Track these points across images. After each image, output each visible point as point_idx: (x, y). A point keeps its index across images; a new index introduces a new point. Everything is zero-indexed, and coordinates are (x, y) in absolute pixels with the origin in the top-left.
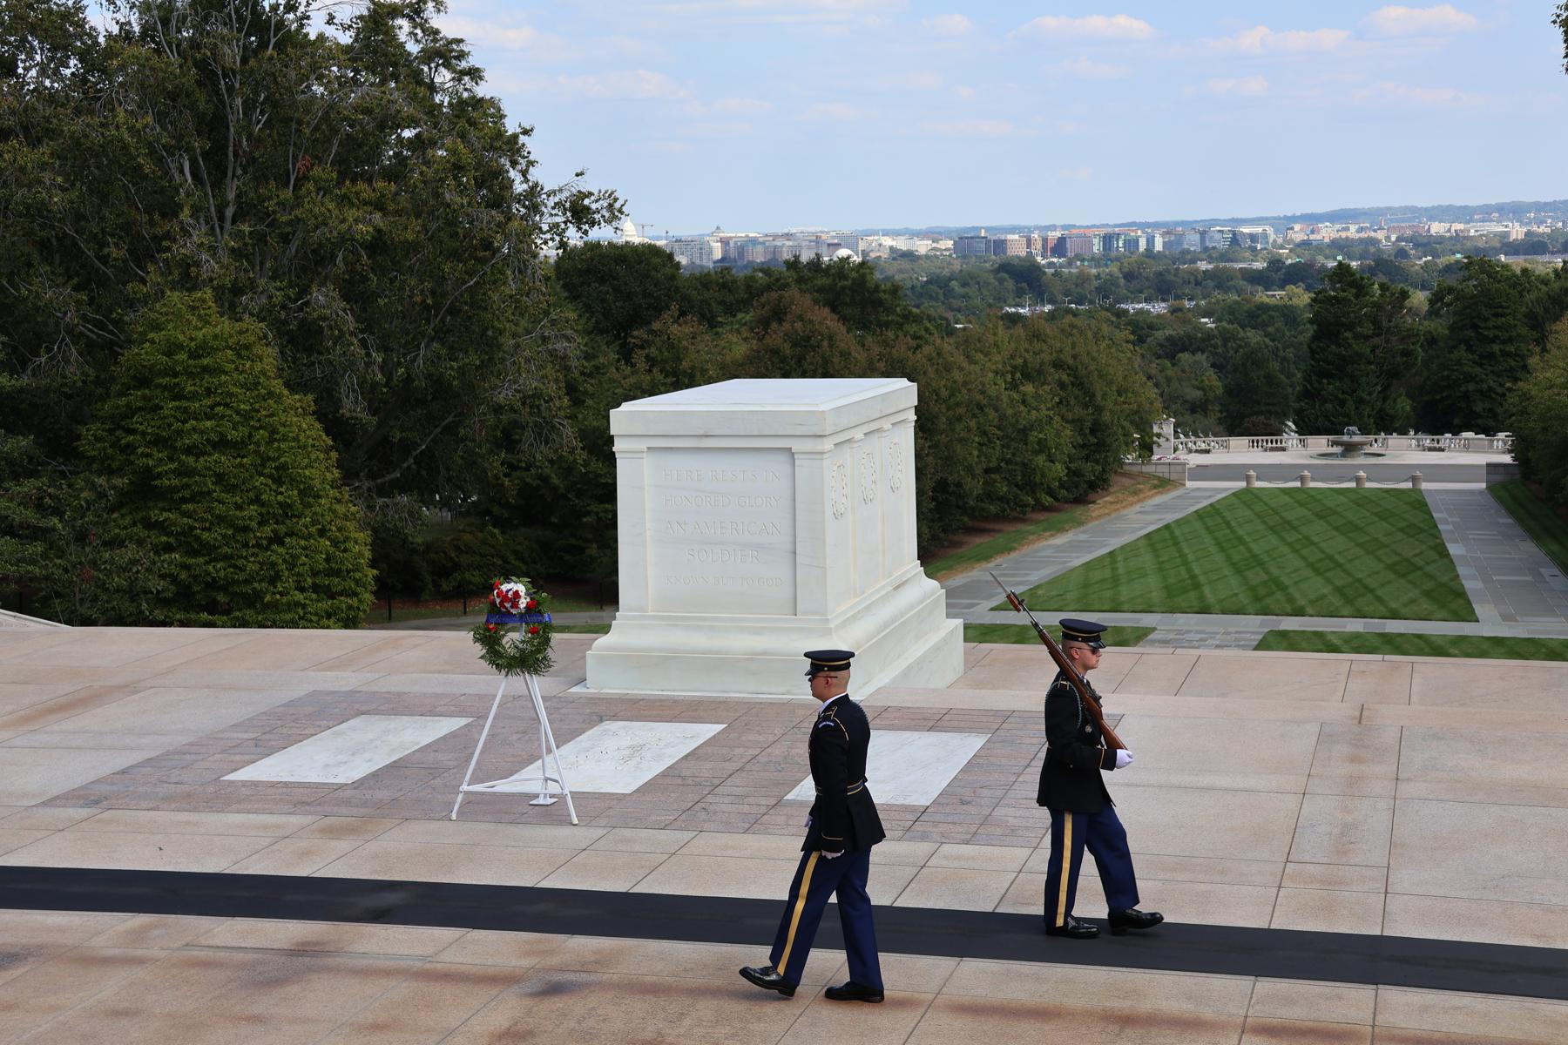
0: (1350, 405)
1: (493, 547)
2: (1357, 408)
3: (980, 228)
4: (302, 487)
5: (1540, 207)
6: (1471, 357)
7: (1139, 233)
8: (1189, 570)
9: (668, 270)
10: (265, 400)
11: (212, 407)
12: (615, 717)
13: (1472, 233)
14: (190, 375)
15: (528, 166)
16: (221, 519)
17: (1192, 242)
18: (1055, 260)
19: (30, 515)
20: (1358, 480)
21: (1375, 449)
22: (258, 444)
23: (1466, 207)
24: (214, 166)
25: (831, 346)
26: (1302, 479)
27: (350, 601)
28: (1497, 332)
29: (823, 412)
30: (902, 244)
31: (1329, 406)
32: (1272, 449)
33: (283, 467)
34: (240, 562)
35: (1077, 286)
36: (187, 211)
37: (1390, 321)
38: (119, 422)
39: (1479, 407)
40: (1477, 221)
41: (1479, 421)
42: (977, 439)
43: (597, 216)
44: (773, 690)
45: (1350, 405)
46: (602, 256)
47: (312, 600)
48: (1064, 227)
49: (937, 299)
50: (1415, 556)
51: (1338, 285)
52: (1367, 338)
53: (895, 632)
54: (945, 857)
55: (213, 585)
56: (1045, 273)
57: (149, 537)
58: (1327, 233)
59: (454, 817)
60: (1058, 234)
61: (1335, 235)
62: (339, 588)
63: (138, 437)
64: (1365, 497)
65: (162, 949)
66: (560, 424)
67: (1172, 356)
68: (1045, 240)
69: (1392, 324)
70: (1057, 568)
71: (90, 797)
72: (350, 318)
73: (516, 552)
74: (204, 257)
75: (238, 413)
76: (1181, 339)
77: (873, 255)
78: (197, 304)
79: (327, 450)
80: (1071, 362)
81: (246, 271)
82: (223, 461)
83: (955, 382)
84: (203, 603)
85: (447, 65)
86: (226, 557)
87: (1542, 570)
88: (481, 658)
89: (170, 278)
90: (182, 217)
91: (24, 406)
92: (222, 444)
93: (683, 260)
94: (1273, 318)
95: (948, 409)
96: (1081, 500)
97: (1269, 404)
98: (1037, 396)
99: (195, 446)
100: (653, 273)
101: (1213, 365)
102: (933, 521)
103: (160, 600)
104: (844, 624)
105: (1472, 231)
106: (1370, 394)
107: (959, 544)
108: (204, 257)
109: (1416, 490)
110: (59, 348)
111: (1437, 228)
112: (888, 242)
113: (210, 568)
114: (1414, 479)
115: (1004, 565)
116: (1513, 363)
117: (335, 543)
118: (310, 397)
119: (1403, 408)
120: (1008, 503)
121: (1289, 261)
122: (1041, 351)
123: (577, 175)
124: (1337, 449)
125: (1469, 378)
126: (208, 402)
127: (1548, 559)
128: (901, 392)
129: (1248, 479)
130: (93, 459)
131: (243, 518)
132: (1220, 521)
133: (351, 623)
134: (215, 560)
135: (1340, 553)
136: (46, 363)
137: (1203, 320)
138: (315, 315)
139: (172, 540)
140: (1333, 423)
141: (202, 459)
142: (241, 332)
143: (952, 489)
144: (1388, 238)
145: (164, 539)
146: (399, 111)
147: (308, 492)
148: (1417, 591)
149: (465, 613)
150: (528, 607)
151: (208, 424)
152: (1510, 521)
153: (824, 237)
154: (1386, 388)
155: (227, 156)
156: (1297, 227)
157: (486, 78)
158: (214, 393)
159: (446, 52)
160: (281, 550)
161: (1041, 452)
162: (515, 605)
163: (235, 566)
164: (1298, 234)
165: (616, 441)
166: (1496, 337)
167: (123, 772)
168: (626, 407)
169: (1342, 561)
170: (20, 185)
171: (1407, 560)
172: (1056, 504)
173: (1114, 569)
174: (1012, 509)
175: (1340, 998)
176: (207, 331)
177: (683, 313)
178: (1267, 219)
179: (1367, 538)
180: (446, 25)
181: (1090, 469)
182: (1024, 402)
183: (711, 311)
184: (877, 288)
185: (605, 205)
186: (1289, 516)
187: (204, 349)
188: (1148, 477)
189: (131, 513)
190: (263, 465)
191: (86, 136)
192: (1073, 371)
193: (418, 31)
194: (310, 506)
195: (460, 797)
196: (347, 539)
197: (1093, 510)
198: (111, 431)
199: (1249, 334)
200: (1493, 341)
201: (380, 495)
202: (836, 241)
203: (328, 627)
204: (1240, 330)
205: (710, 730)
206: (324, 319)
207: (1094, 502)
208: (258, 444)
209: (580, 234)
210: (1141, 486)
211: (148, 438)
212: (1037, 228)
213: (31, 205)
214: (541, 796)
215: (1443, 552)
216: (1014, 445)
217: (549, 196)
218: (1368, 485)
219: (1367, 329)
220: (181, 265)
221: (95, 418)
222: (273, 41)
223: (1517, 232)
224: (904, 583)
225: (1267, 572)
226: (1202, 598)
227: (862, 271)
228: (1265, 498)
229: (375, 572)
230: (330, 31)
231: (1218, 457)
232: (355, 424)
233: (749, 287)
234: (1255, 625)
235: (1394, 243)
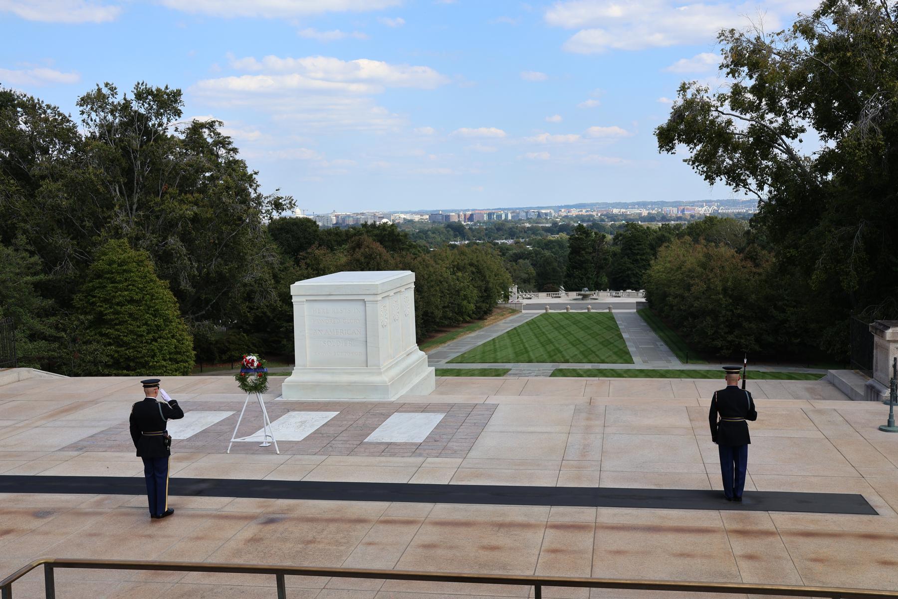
0: (585, 280)
2: (587, 281)
3: (439, 211)
4: (165, 318)
5: (653, 203)
6: (629, 261)
7: (502, 212)
8: (524, 346)
10: (149, 283)
11: (127, 286)
12: (294, 410)
13: (628, 213)
14: (119, 273)
15: (256, 187)
16: (132, 332)
17: (522, 215)
18: (469, 223)
19: (53, 332)
20: (588, 309)
21: (595, 297)
22: (146, 301)
23: (626, 203)
24: (129, 189)
25: (380, 258)
26: (567, 309)
27: (185, 365)
28: (638, 251)
29: (377, 284)
30: (408, 217)
31: (576, 280)
32: (555, 297)
33: (157, 310)
34: (139, 349)
35: (478, 233)
36: (117, 207)
37: (599, 247)
38: (90, 293)
39: (633, 280)
40: (630, 208)
41: (633, 286)
42: (439, 295)
43: (285, 207)
44: (358, 397)
45: (585, 280)
46: (287, 223)
47: (169, 364)
48: (473, 210)
49: (423, 239)
50: (611, 338)
51: (579, 233)
52: (590, 253)
53: (409, 372)
54: (429, 463)
55: (128, 359)
56: (465, 228)
57: (102, 339)
58: (574, 212)
59: (228, 452)
60: (470, 213)
61: (577, 213)
62: (180, 359)
63: (97, 299)
64: (591, 316)
65: (109, 509)
67: (516, 261)
68: (465, 215)
69: (600, 248)
71: (77, 447)
72: (184, 249)
74: (124, 225)
75: (138, 288)
76: (519, 254)
77: (397, 221)
79: (175, 303)
80: (476, 263)
81: (141, 230)
82: (132, 308)
83: (430, 272)
85: (224, 147)
86: (133, 347)
87: (657, 343)
88: (239, 387)
89: (110, 234)
90: (115, 209)
91: (50, 287)
92: (131, 301)
93: (320, 224)
94: (554, 245)
95: (428, 283)
96: (481, 318)
97: (553, 280)
98: (463, 277)
100: (308, 229)
101: (532, 264)
102: (422, 327)
103: (107, 366)
104: (387, 370)
105: (628, 212)
106: (592, 275)
107: (433, 337)
108: (124, 225)
109: (610, 313)
110: (65, 263)
111: (615, 211)
112: (403, 216)
114: (609, 308)
115: (451, 345)
116: (645, 263)
117: (178, 341)
118: (168, 281)
119: (604, 281)
120: (452, 320)
121: (560, 223)
122: (464, 259)
123: (277, 190)
124: (580, 297)
125: (629, 269)
126: (126, 284)
127: (659, 338)
128: (409, 276)
129: (546, 309)
130: (79, 308)
131: (140, 331)
132: (536, 326)
133: (185, 373)
134: (128, 349)
135: (582, 338)
136: (60, 269)
137: (528, 247)
138: (170, 248)
139: (111, 341)
140: (578, 287)
141: (123, 308)
142: (139, 256)
143: (430, 315)
144: (597, 215)
145: (108, 340)
146: (204, 166)
147: (167, 321)
148: (611, 352)
149: (232, 368)
151: (126, 293)
152: (645, 324)
153: (377, 214)
154: (598, 273)
155: (134, 184)
156: (563, 210)
157: (240, 152)
158: (128, 280)
159: (223, 142)
160: (156, 344)
161: (465, 299)
163: (137, 351)
164: (563, 213)
166: (638, 253)
167: (92, 436)
168: (297, 283)
169: (583, 341)
170: (49, 197)
171: (607, 340)
172: (471, 320)
173: (495, 346)
174: (454, 322)
175: (583, 512)
176: (125, 255)
177: (320, 245)
178: (551, 207)
179: (592, 332)
180: (223, 131)
181: (484, 306)
182: (458, 279)
183: (332, 245)
184: (398, 235)
185: (288, 202)
186: (562, 323)
187: (124, 262)
188: (507, 309)
189: (94, 330)
190: (149, 310)
191: (76, 178)
192: (477, 267)
193: (212, 134)
194: (168, 326)
195: (231, 444)
196: (183, 339)
197: (486, 322)
198: (86, 297)
199: (545, 252)
200: (638, 254)
201: (197, 321)
202: (382, 216)
203: (176, 375)
204: (542, 251)
205: (333, 414)
206: (174, 249)
207: (486, 319)
208: (146, 301)
209: (278, 214)
210: (505, 313)
211: (101, 299)
212: (462, 210)
214: (264, 443)
215: (621, 337)
216: (454, 297)
217: (265, 199)
218: (592, 311)
219: (590, 250)
220: (115, 229)
221: (79, 291)
222: (153, 138)
223: (645, 213)
224: (411, 353)
225: (554, 346)
226: (529, 357)
227: (392, 228)
228: (553, 317)
229: (195, 352)
230: (176, 134)
231: (535, 301)
232: (186, 292)
233: (347, 234)
234: (550, 367)
235: (599, 217)
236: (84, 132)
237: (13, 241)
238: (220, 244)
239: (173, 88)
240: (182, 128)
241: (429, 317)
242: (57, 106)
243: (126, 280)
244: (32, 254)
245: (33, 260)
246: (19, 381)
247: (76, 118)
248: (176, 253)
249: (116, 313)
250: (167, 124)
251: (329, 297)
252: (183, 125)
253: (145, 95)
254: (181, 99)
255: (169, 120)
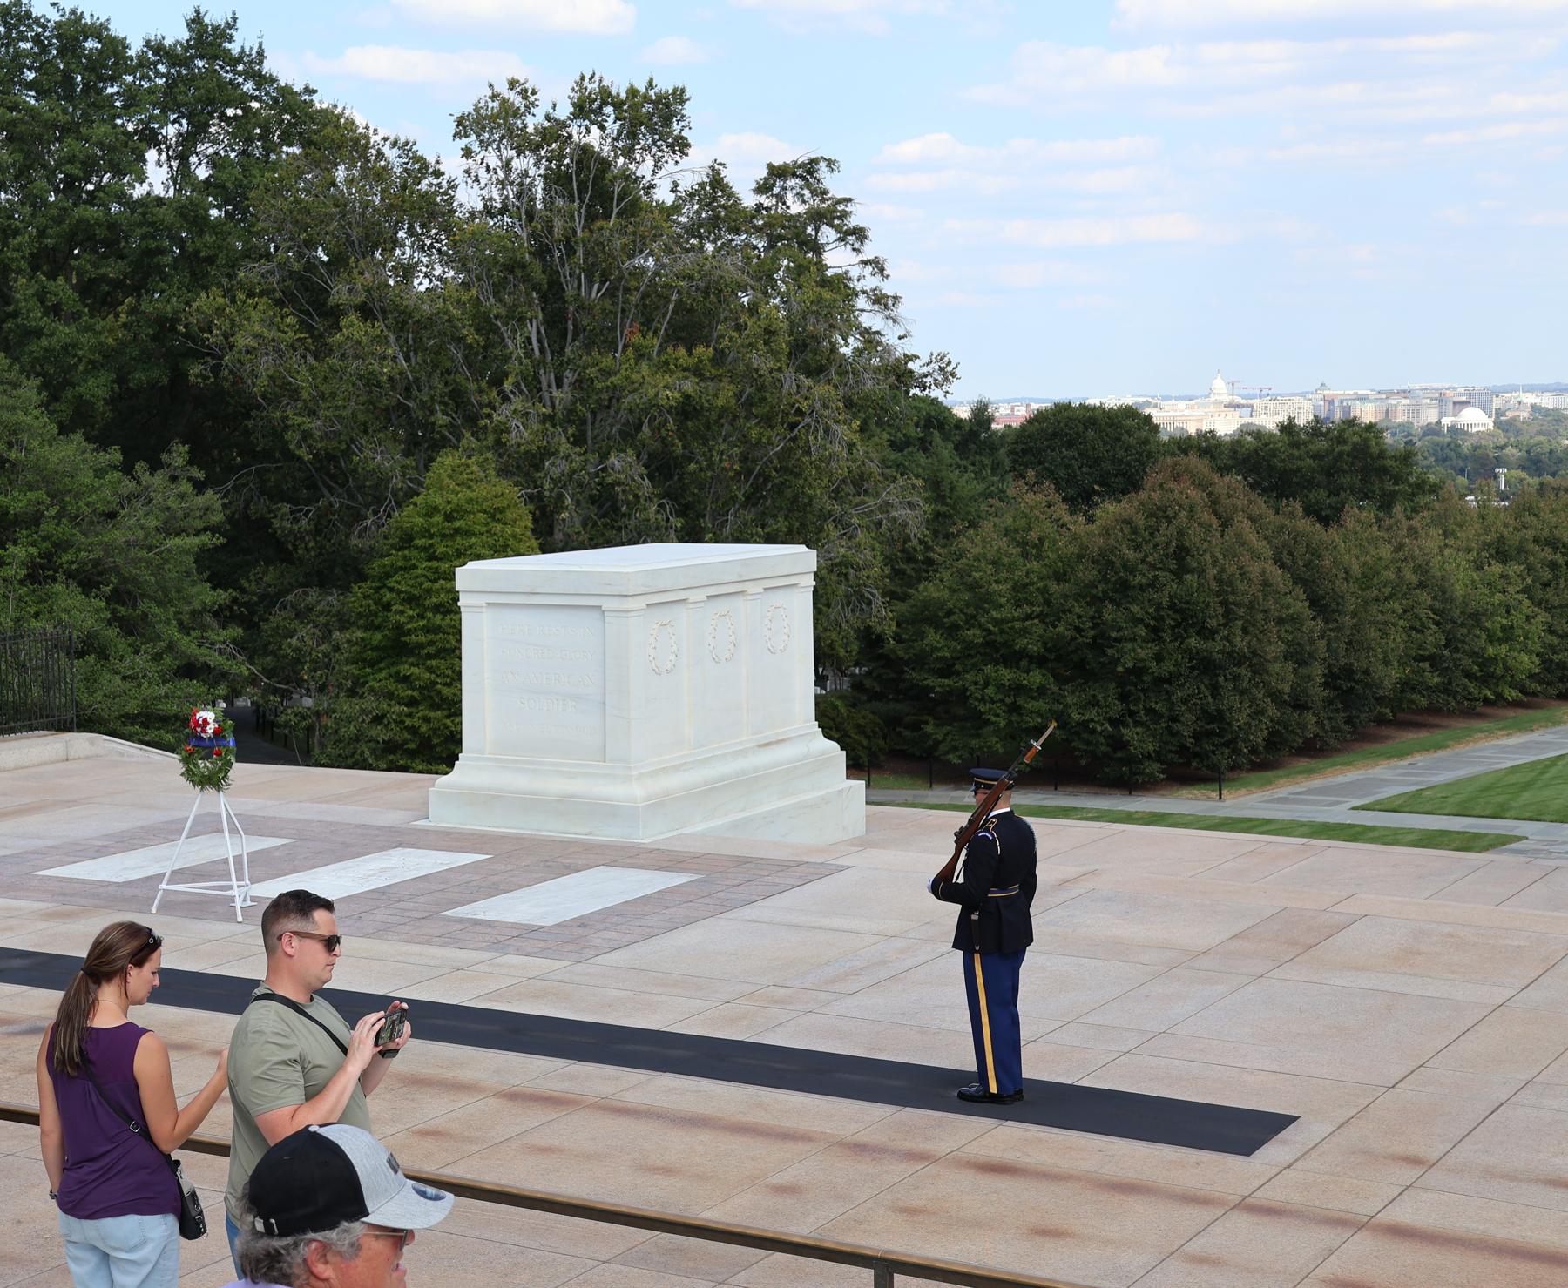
1: (833, 719)
9: (1143, 434)
14: (444, 536)
25: (1191, 516)
30: (1547, 401)
36: (511, 379)
43: (928, 380)
59: (154, 911)
63: (394, 595)
66: (871, 593)
70: (1485, 768)
73: (858, 726)
77: (1510, 414)
78: (462, 469)
84: (444, 755)
99: (441, 605)
107: (1387, 738)
110: (385, 511)
112: (1530, 399)
113: (448, 722)
120: (1454, 698)
138: (609, 480)
139: (416, 694)
141: (448, 617)
143: (1357, 677)
150: (216, 732)
153: (1449, 393)
159: (830, 213)
162: (204, 731)
165: (461, 596)
168: (471, 565)
170: (357, 357)
172: (1525, 699)
180: (835, 185)
184: (1382, 454)
189: (389, 668)
198: (377, 590)
202: (1464, 399)
206: (619, 484)
211: (402, 595)
212: (1004, 401)
213: (363, 376)
222: (616, 210)
224: (783, 740)
236: (468, 198)
237: (164, 457)
238: (749, 472)
239: (665, 85)
240: (687, 183)
241: (1357, 682)
242: (411, 140)
243: (457, 550)
244: (200, 487)
245: (200, 500)
246: (67, 760)
247: (453, 166)
248: (624, 491)
249: (436, 630)
250: (654, 173)
251: (529, 601)
252: (689, 176)
253: (595, 105)
254: (684, 112)
255: (657, 165)
